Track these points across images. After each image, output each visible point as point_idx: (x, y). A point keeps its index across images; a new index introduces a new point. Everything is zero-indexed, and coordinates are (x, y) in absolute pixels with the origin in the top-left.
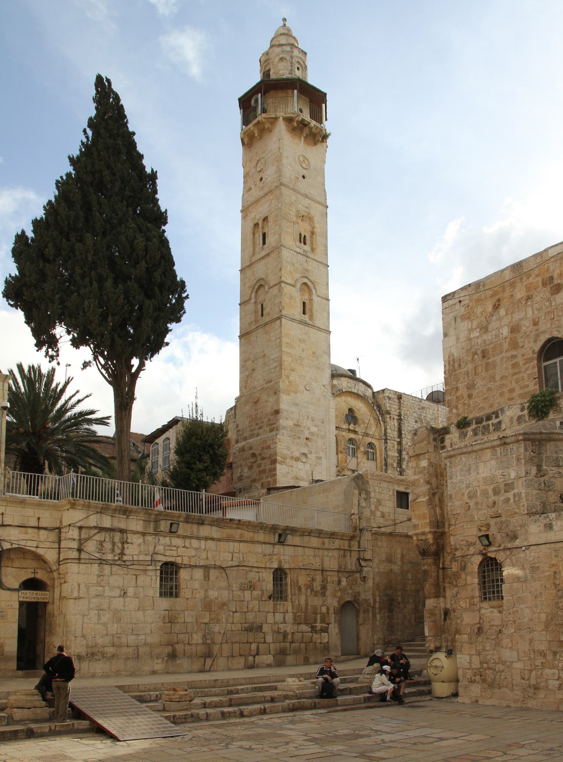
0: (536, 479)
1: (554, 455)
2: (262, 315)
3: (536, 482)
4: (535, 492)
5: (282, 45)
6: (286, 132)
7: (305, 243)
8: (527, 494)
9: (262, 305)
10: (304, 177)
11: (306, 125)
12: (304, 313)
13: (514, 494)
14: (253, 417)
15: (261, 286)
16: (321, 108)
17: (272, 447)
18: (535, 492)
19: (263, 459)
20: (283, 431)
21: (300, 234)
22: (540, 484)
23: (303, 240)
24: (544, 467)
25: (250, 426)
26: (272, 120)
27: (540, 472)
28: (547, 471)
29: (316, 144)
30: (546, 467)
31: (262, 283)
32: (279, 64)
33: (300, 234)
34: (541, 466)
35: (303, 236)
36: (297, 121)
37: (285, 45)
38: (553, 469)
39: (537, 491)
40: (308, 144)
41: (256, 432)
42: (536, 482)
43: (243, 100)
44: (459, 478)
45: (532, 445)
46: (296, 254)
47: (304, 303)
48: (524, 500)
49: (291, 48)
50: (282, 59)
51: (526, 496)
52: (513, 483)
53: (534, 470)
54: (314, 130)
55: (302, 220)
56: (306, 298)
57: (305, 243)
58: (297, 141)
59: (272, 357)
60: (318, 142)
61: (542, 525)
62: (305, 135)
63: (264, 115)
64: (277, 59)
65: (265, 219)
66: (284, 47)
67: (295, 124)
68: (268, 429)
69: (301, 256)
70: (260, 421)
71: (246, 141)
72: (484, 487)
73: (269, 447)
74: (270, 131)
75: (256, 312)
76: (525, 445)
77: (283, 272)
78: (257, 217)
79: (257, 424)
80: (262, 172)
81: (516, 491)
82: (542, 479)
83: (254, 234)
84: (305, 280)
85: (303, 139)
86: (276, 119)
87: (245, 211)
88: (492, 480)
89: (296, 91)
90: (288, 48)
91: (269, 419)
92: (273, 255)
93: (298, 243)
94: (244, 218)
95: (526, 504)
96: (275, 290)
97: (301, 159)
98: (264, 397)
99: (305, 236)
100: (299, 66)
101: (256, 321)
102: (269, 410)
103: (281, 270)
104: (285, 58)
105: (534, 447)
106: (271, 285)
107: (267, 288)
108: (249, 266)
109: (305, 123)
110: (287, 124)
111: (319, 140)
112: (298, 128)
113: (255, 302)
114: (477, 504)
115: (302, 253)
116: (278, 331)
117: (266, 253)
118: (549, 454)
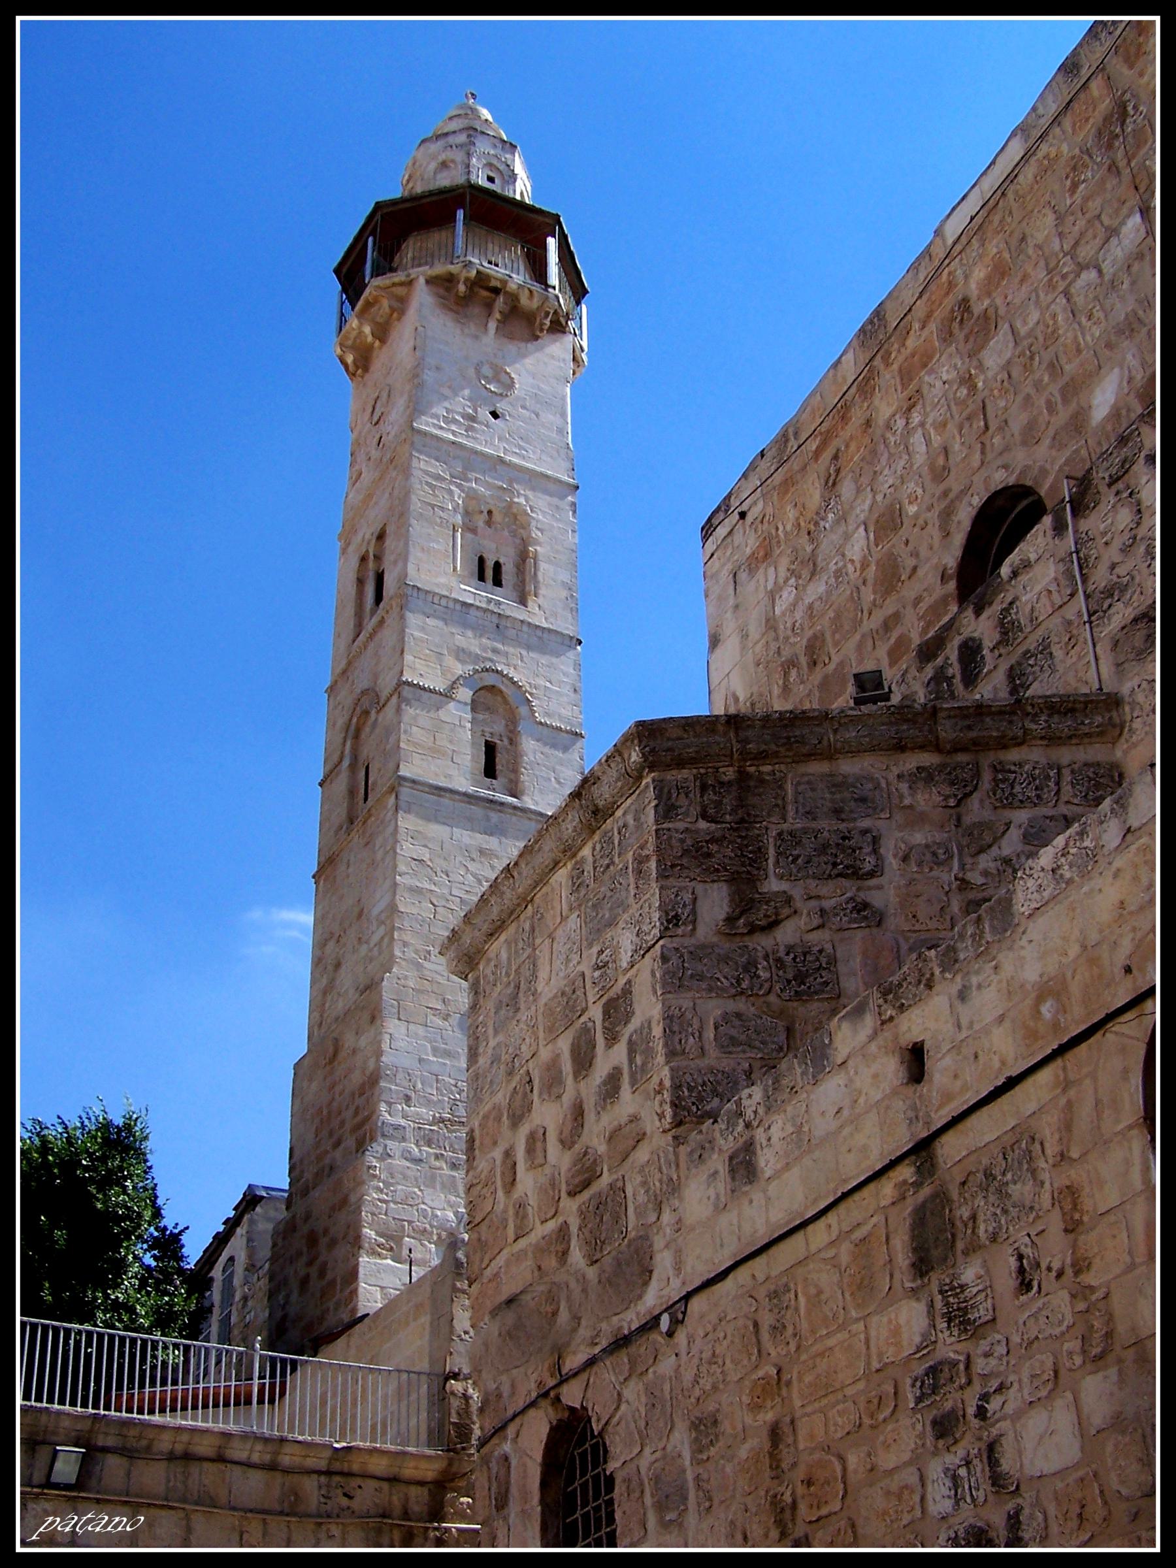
0: (726, 946)
1: (827, 825)
2: (366, 799)
3: (725, 959)
4: (714, 1009)
5: (446, 134)
6: (438, 311)
7: (497, 582)
8: (673, 1023)
9: (367, 768)
10: (495, 415)
11: (496, 291)
12: (490, 771)
13: (630, 1041)
14: (325, 1112)
15: (366, 713)
16: (544, 247)
17: (353, 1198)
18: (714, 1009)
19: (333, 1243)
20: (389, 1142)
21: (481, 561)
22: (750, 967)
23: (488, 572)
24: (773, 885)
25: (318, 1144)
26: (401, 291)
27: (751, 913)
28: (789, 900)
29: (537, 338)
30: (784, 886)
31: (365, 702)
32: (439, 176)
33: (481, 561)
34: (752, 881)
35: (490, 564)
36: (467, 279)
37: (454, 132)
38: (825, 889)
39: (731, 1006)
40: (511, 337)
41: (327, 1161)
42: (725, 959)
43: (344, 270)
44: (492, 1043)
45: (704, 788)
46: (458, 607)
47: (490, 750)
48: (660, 1059)
49: (469, 136)
50: (444, 165)
51: (668, 1033)
52: (627, 991)
53: (714, 903)
54: (524, 301)
55: (489, 523)
56: (497, 728)
57: (497, 582)
58: (472, 328)
59: (375, 912)
60: (542, 330)
61: (723, 1168)
62: (498, 316)
63: (378, 281)
64: (433, 166)
65: (381, 537)
66: (451, 140)
67: (462, 288)
68: (350, 1142)
69: (479, 614)
70: (335, 1123)
71: (350, 359)
72: (545, 1054)
73: (345, 1201)
74: (399, 319)
75: (352, 793)
76: (659, 786)
77: (408, 658)
78: (367, 536)
79: (331, 1134)
80: (381, 422)
81: (635, 1023)
82: (763, 942)
83: (360, 582)
84: (490, 679)
85: (492, 325)
86: (410, 283)
87: (346, 537)
88: (569, 1004)
89: (460, 214)
90: (462, 138)
91: (356, 1113)
92: (389, 621)
93: (475, 581)
94: (344, 551)
95: (666, 1072)
96: (390, 710)
97: (486, 370)
98: (349, 1040)
99: (497, 566)
100: (492, 174)
101: (351, 820)
102: (357, 1078)
103: (402, 652)
104: (453, 161)
105: (711, 796)
106: (382, 702)
107: (373, 712)
108: (344, 672)
109: (493, 283)
110: (442, 291)
111: (542, 324)
112: (473, 297)
113: (353, 767)
114: (532, 1138)
115: (484, 605)
116: (391, 829)
117: (379, 618)
118: (793, 822)
